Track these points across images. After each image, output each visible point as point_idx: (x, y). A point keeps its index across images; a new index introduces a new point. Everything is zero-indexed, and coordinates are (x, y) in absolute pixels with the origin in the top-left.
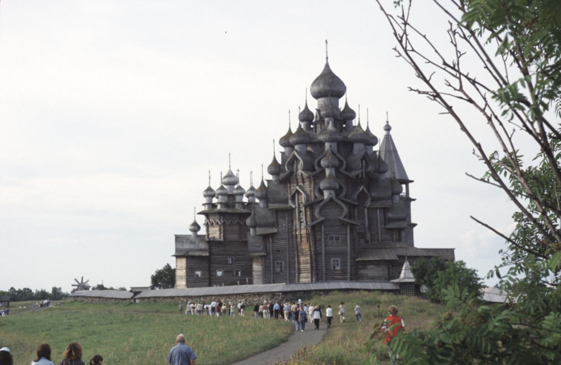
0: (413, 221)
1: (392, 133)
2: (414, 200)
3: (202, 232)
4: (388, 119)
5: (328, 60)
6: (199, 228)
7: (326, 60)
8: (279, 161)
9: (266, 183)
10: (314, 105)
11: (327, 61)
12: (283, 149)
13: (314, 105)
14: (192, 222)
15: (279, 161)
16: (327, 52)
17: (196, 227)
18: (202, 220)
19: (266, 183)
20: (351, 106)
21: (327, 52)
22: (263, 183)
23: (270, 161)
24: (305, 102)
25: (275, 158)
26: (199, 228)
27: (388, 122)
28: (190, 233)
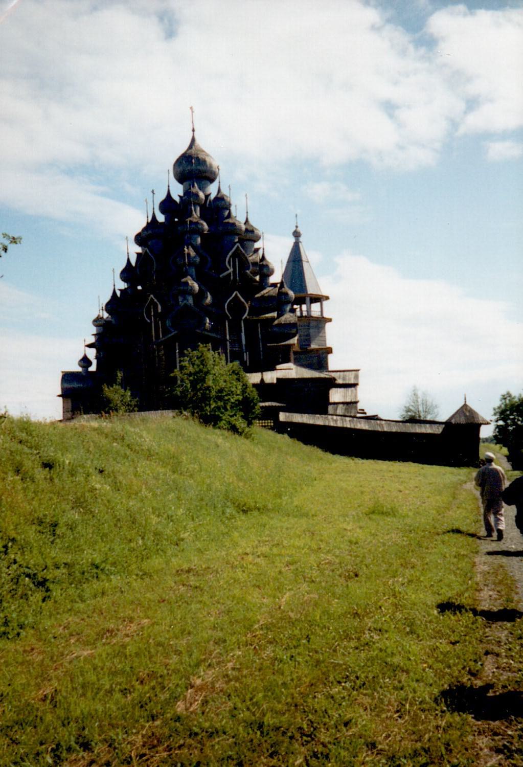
0: (328, 345)
1: (301, 239)
2: (330, 320)
3: (93, 368)
4: (297, 223)
5: (195, 133)
6: (90, 363)
7: (192, 133)
8: (133, 263)
9: (118, 293)
10: (177, 191)
11: (193, 134)
12: (139, 250)
13: (177, 191)
14: (81, 357)
15: (133, 263)
16: (193, 123)
17: (85, 361)
18: (92, 354)
19: (118, 293)
20: (225, 191)
21: (193, 123)
22: (114, 292)
23: (123, 265)
24: (167, 188)
25: (128, 260)
26: (90, 363)
27: (297, 227)
28: (80, 369)
